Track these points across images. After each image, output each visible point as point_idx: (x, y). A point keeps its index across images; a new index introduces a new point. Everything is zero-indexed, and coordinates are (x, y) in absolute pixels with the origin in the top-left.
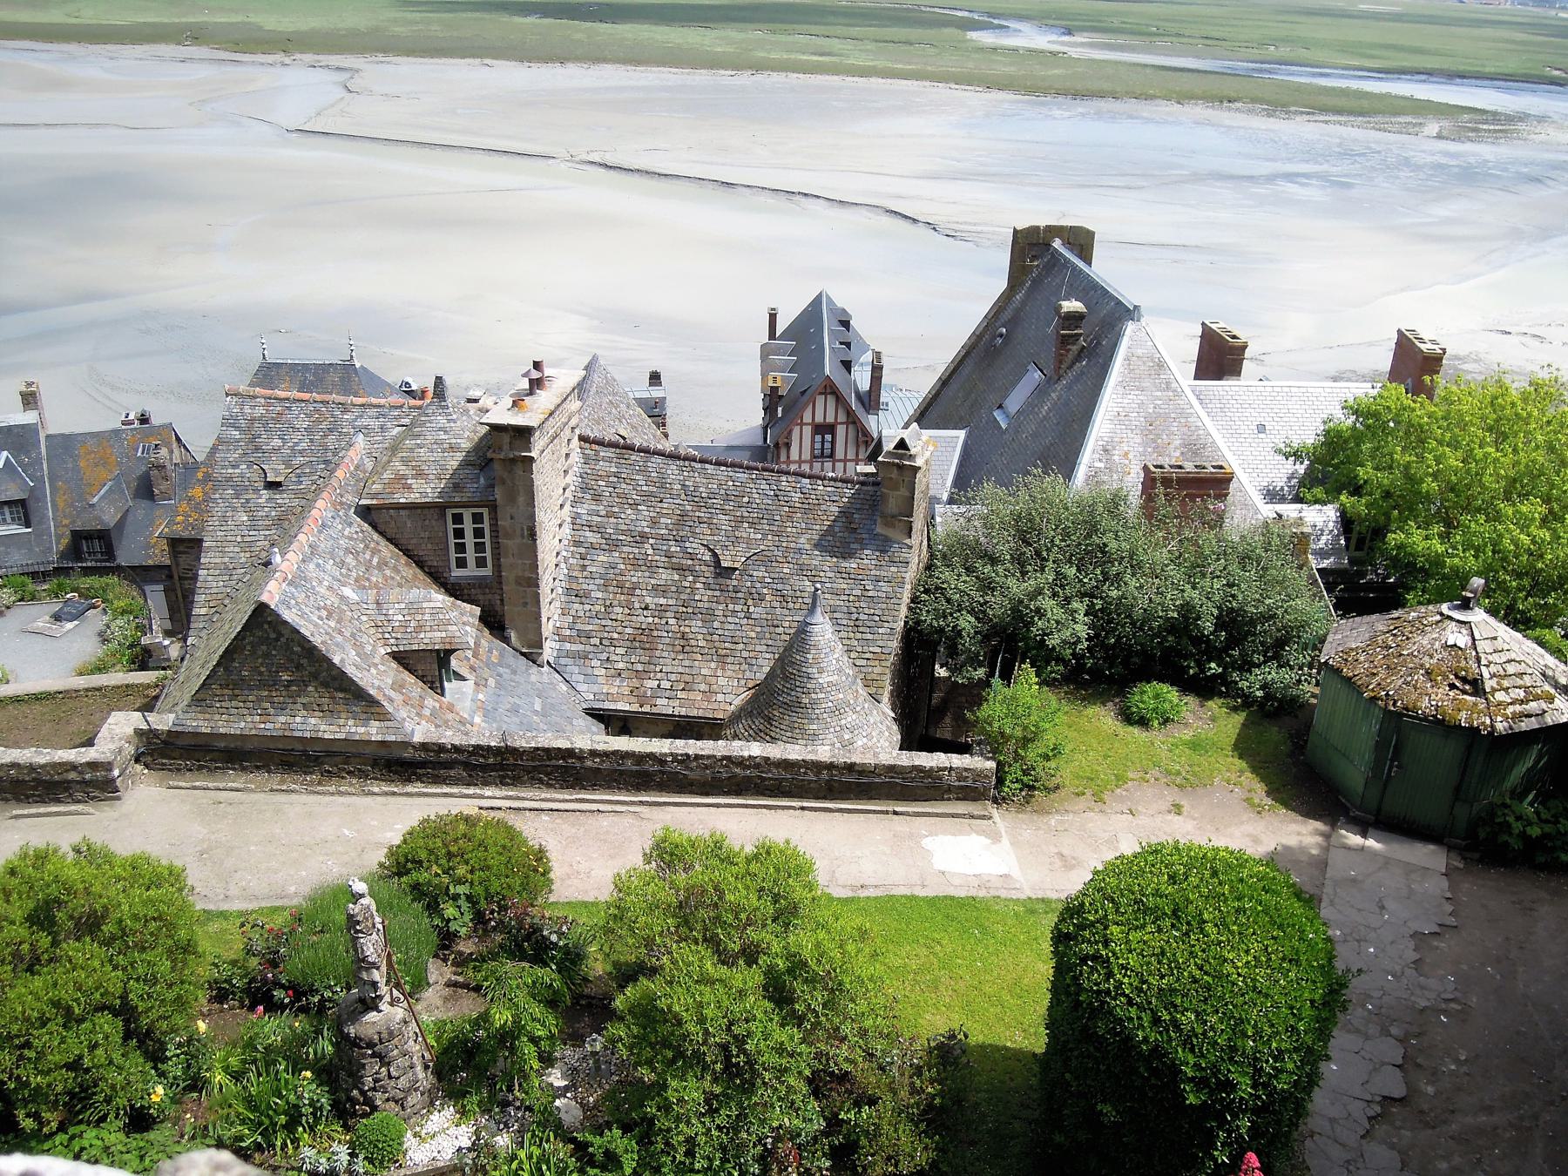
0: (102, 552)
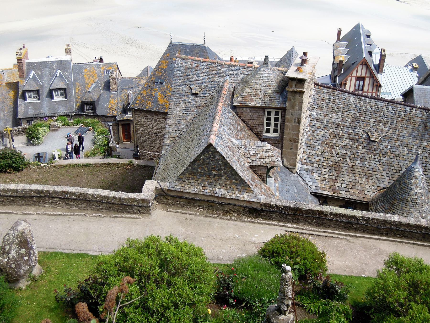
0: (91, 110)
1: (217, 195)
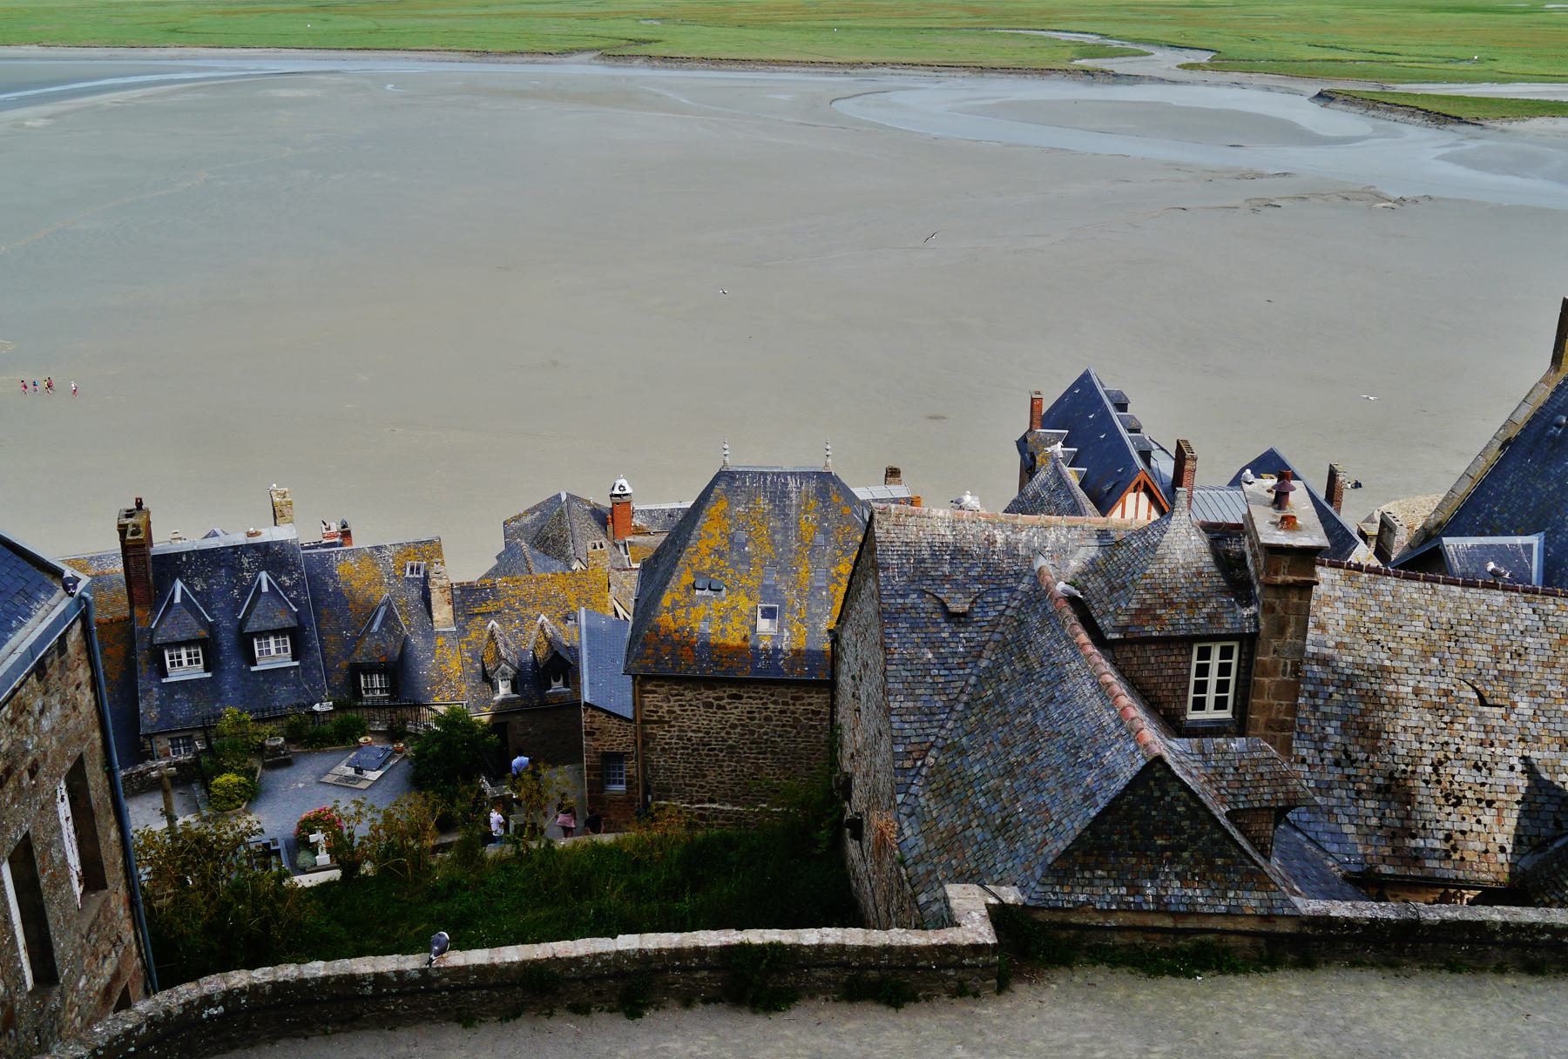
1: (1173, 908)
